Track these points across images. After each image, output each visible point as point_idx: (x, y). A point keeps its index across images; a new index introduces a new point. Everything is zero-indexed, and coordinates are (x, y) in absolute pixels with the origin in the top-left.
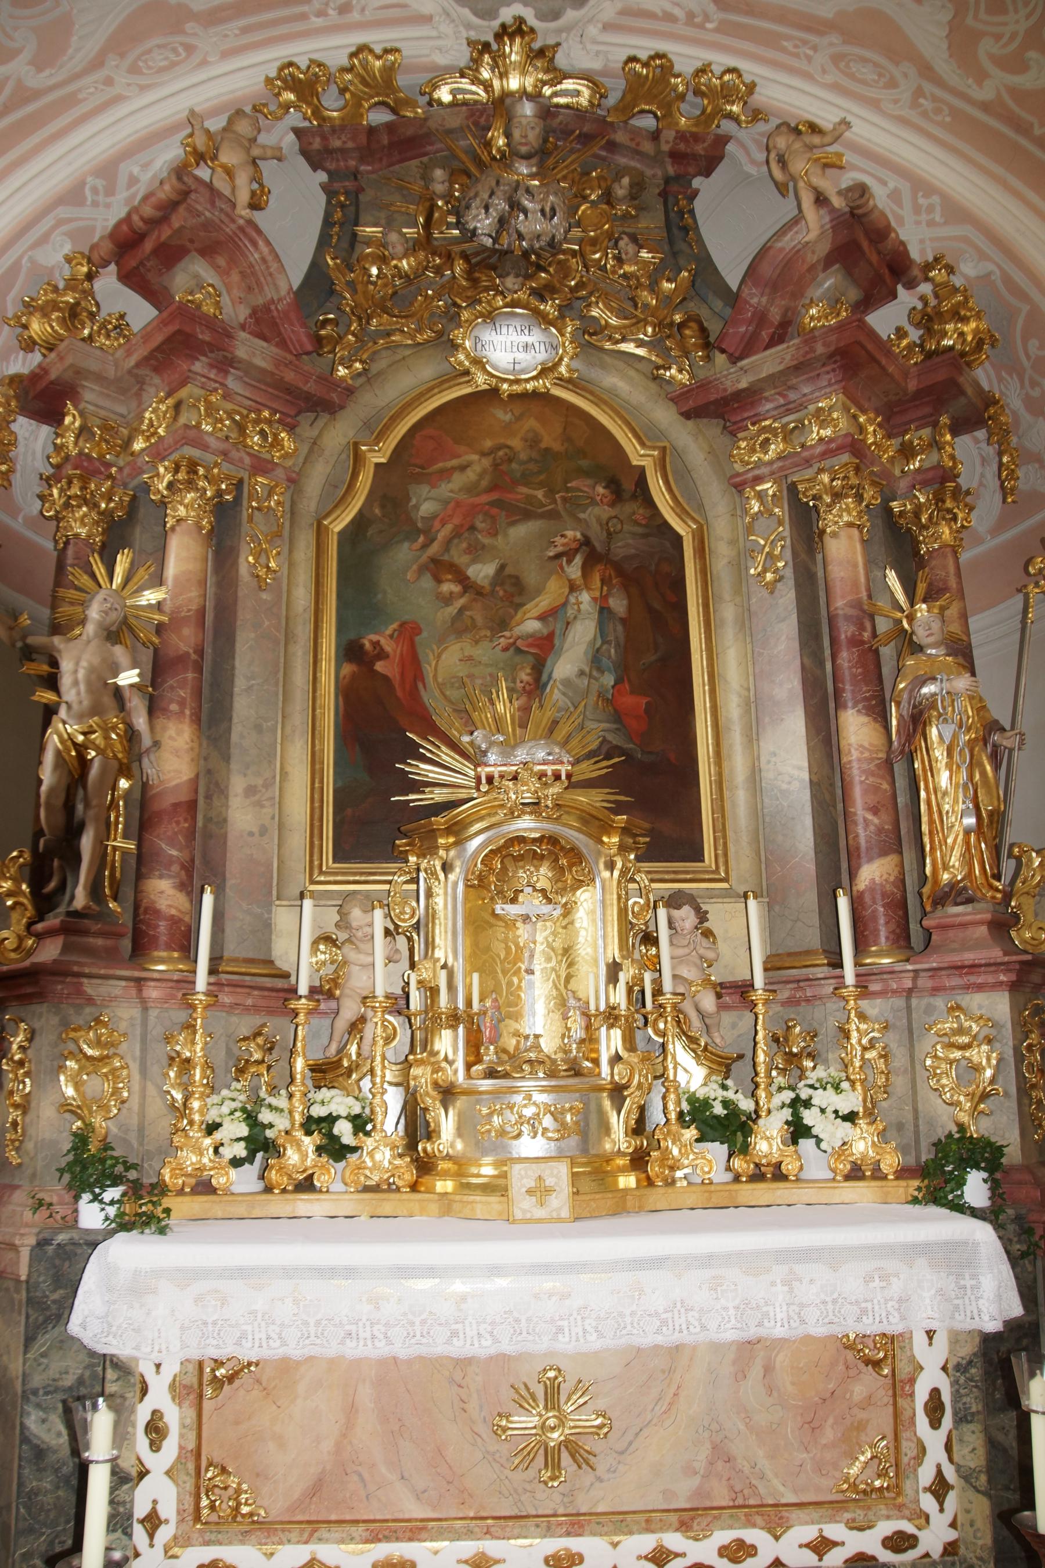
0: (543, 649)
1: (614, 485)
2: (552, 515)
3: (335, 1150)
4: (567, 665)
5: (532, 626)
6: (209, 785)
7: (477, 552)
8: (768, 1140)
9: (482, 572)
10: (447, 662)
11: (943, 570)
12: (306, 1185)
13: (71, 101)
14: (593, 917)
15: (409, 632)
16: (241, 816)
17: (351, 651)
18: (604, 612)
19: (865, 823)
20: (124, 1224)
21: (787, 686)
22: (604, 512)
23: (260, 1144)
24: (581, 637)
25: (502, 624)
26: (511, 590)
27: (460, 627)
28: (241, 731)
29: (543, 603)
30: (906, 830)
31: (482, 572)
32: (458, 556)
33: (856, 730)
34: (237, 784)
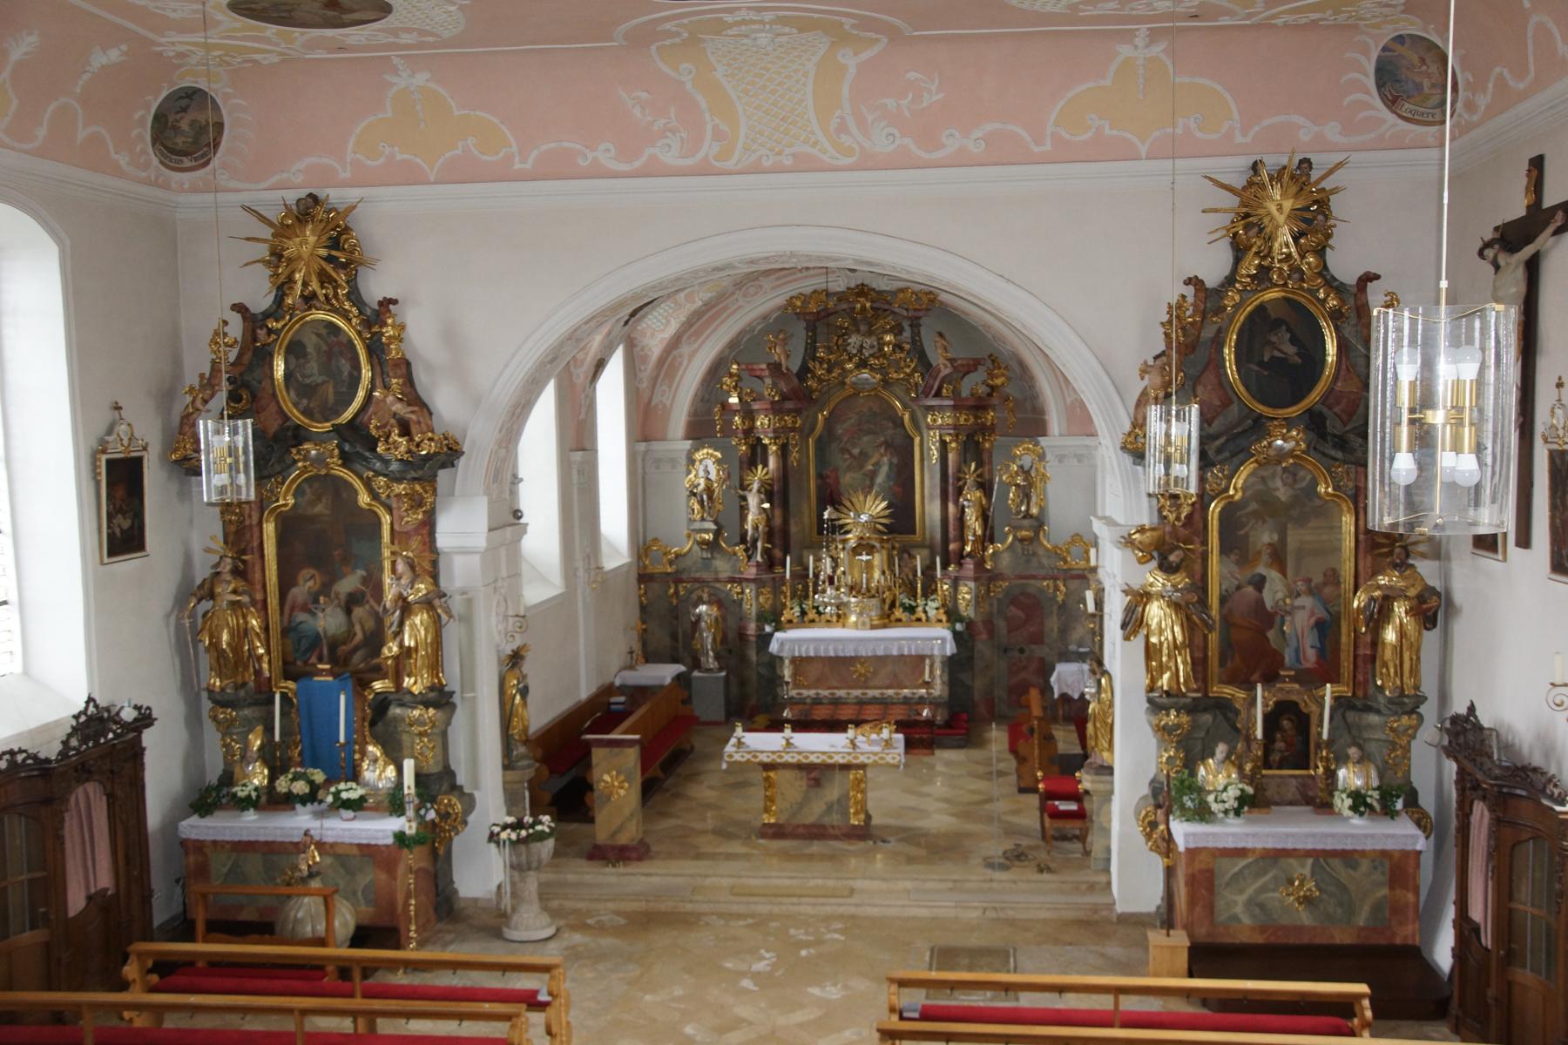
0: (873, 475)
1: (894, 423)
2: (875, 433)
3: (819, 613)
4: (880, 479)
5: (870, 467)
6: (786, 522)
7: (854, 445)
8: (920, 613)
9: (856, 451)
10: (847, 479)
11: (985, 457)
12: (813, 621)
13: (725, 308)
14: (878, 560)
15: (836, 470)
16: (793, 529)
17: (820, 476)
18: (891, 464)
19: (952, 533)
20: (777, 629)
21: (938, 491)
22: (890, 432)
23: (803, 613)
24: (884, 470)
25: (861, 467)
26: (864, 456)
27: (849, 469)
28: (792, 509)
29: (873, 460)
30: (962, 540)
31: (856, 451)
32: (849, 446)
33: (951, 508)
34: (792, 521)
